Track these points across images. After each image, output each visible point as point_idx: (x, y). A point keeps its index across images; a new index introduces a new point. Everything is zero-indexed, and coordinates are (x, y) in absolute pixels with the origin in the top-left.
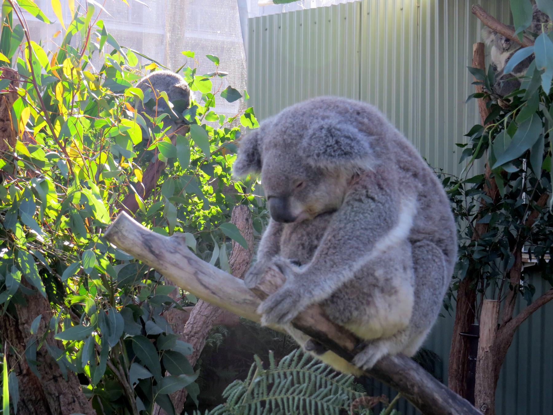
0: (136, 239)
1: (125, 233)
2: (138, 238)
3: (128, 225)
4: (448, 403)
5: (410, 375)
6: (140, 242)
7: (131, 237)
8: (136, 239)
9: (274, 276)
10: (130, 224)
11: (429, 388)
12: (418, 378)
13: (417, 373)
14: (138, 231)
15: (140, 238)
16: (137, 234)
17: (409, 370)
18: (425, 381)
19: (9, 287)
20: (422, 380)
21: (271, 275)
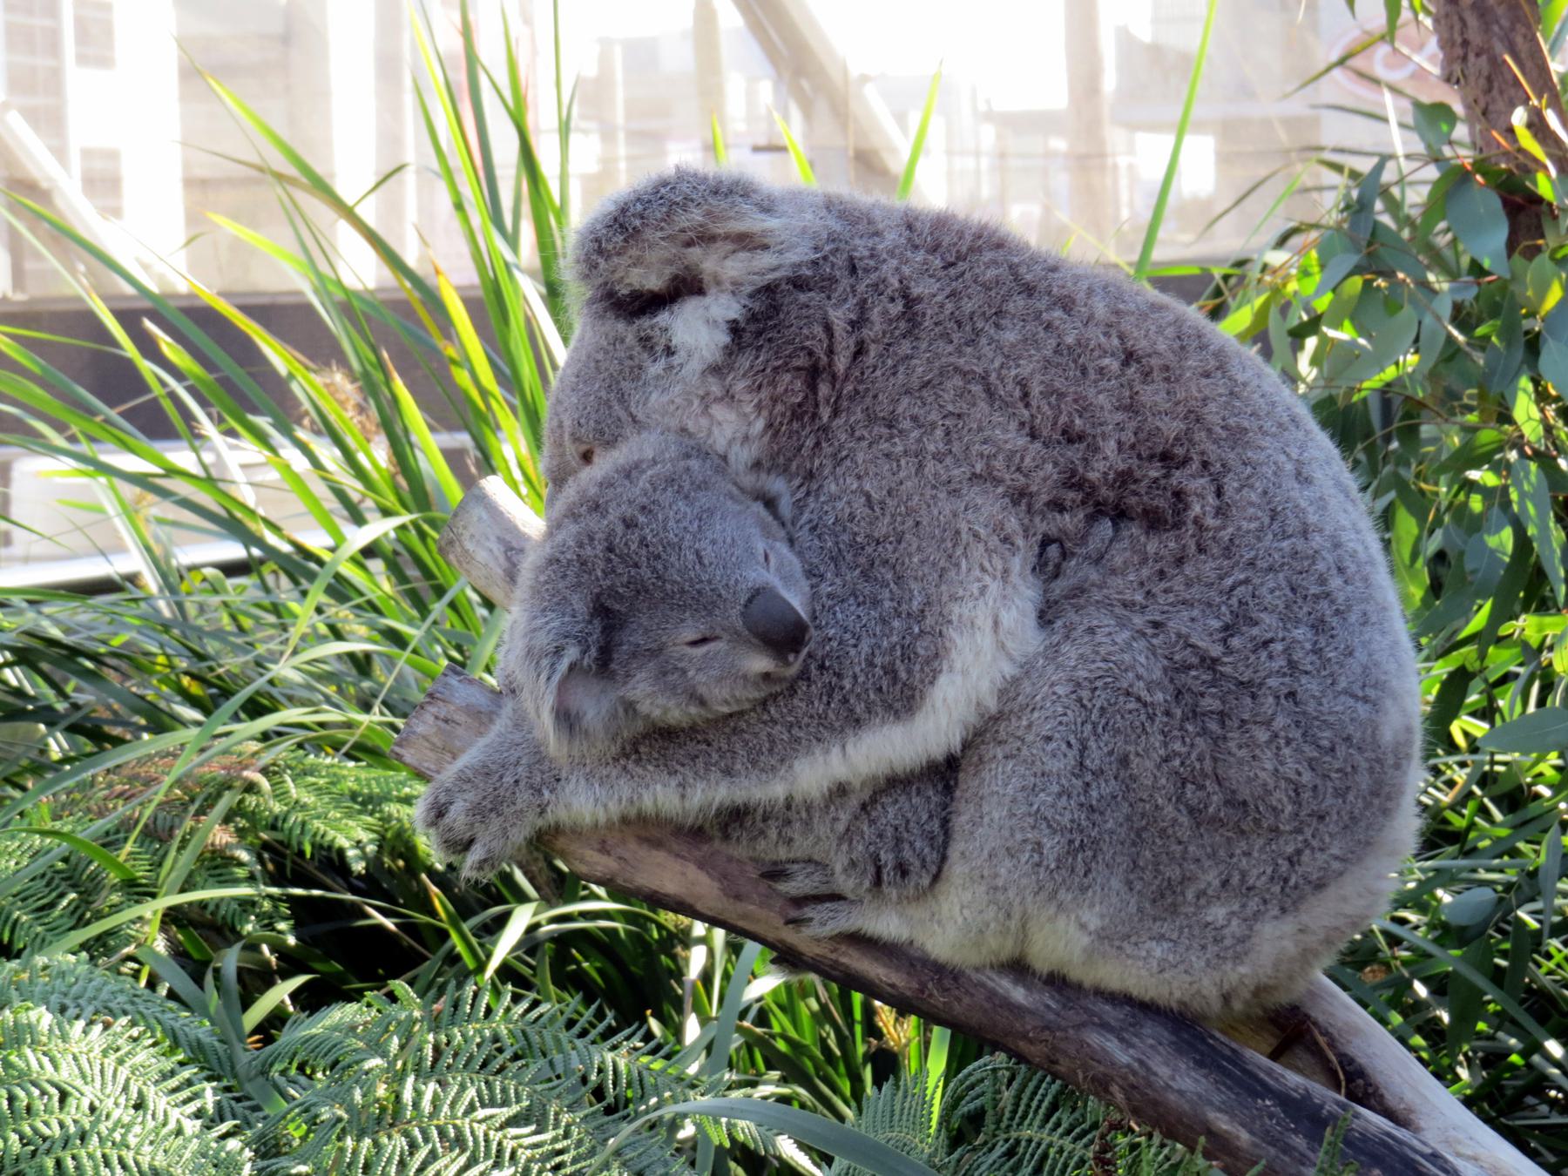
0: (492, 564)
1: (469, 546)
2: (496, 559)
3: (480, 519)
4: (1287, 1149)
5: (1082, 1044)
6: (500, 572)
7: (481, 555)
8: (492, 564)
9: (446, 721)
10: (484, 515)
11: (1181, 1093)
12: (1122, 1056)
13: (1122, 1040)
14: (500, 540)
15: (502, 559)
16: (497, 549)
17: (1079, 1027)
18: (1163, 1071)
19: (1474, 572)
20: (1141, 1062)
21: (437, 718)
